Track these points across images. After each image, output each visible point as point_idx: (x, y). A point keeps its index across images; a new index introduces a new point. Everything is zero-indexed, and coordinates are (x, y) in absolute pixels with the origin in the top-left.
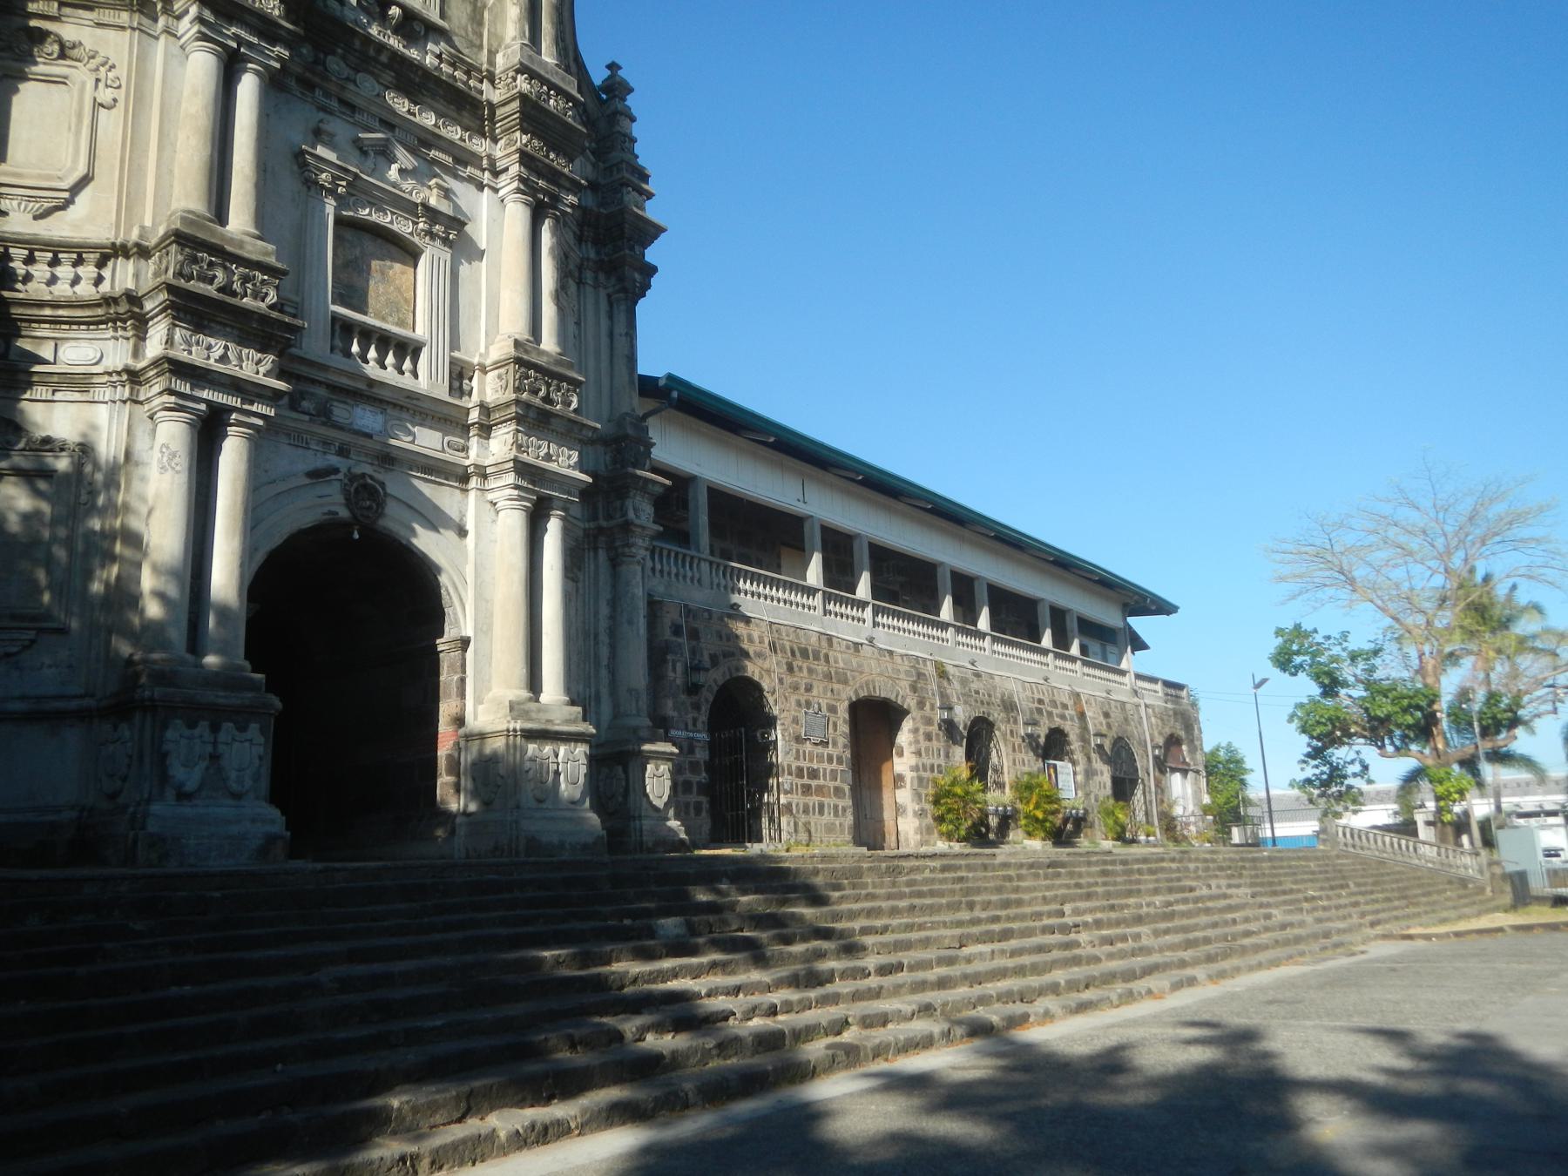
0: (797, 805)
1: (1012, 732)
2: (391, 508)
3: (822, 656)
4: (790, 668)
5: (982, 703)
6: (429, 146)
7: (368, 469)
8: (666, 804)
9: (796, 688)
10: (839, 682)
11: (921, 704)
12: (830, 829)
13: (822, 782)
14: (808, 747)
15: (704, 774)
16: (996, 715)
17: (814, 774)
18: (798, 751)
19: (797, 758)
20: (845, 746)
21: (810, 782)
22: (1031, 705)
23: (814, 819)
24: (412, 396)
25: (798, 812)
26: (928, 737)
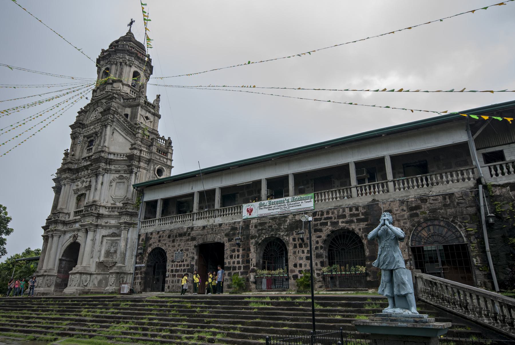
0: (170, 280)
1: (294, 240)
2: (79, 238)
6: (89, 176)
7: (76, 233)
8: (113, 284)
9: (174, 246)
13: (180, 273)
14: (176, 263)
15: (143, 275)
17: (177, 271)
18: (172, 265)
19: (172, 267)
20: (191, 261)
21: (175, 273)
22: (316, 223)
25: (169, 283)
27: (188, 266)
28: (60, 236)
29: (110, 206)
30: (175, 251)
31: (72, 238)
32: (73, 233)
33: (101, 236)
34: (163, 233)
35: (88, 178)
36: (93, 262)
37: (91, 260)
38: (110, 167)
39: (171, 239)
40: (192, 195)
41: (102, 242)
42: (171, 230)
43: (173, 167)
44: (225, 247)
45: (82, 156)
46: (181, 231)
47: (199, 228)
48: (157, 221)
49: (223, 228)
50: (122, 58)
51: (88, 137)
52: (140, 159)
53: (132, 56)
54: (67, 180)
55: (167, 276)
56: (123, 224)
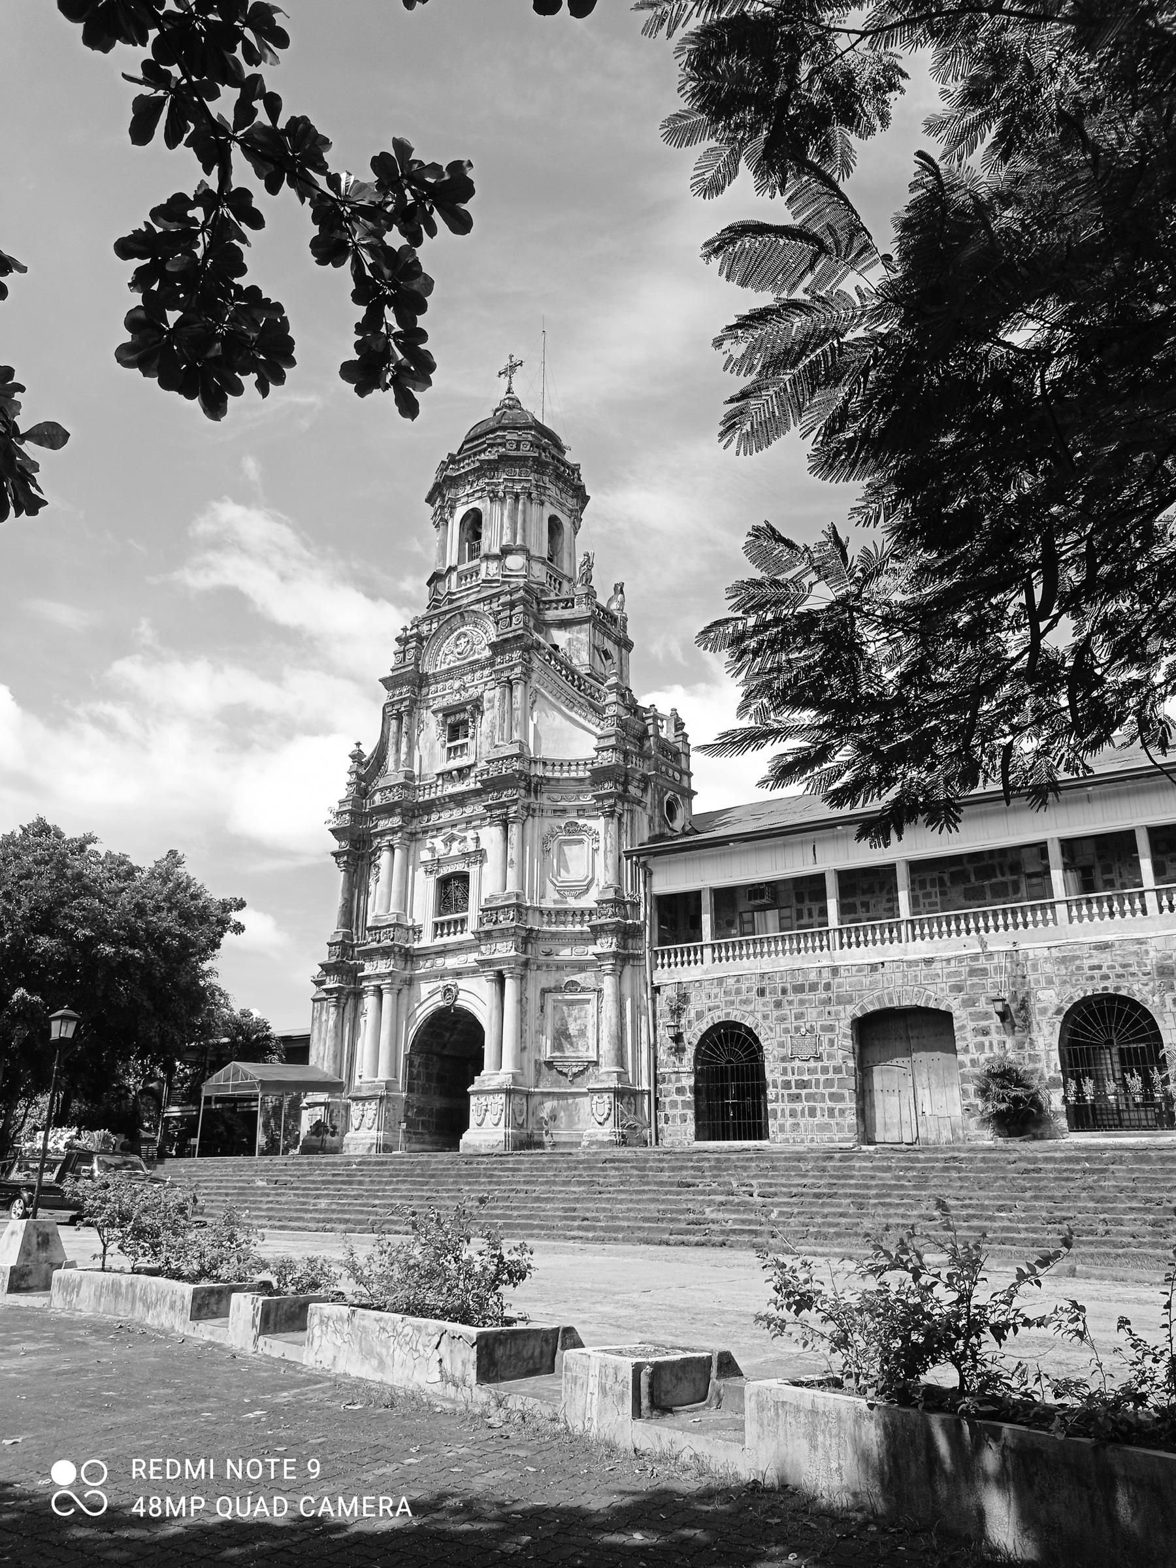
0: (783, 1110)
2: (462, 995)
3: (821, 987)
4: (778, 1004)
5: (1105, 977)
6: (470, 822)
7: (449, 982)
8: (606, 1119)
9: (783, 1019)
10: (839, 1003)
11: (970, 1002)
12: (823, 1128)
13: (813, 1090)
16: (1135, 987)
17: (803, 1084)
19: (785, 1072)
20: (845, 1057)
21: (798, 1091)
23: (802, 1122)
24: (460, 943)
25: (783, 1115)
26: (985, 1032)
27: (840, 1072)
28: (400, 990)
29: (552, 906)
30: (786, 1031)
31: (438, 997)
32: (441, 983)
33: (539, 992)
34: (738, 981)
35: (466, 829)
36: (529, 1061)
37: (525, 1054)
38: (536, 798)
39: (768, 997)
40: (820, 878)
41: (542, 1007)
42: (762, 975)
43: (696, 793)
44: (955, 1021)
45: (431, 766)
46: (800, 980)
47: (859, 971)
48: (708, 952)
49: (940, 972)
50: (520, 481)
51: (448, 712)
52: (626, 776)
53: (543, 474)
54: (399, 835)
55: (770, 1097)
56: (608, 958)
